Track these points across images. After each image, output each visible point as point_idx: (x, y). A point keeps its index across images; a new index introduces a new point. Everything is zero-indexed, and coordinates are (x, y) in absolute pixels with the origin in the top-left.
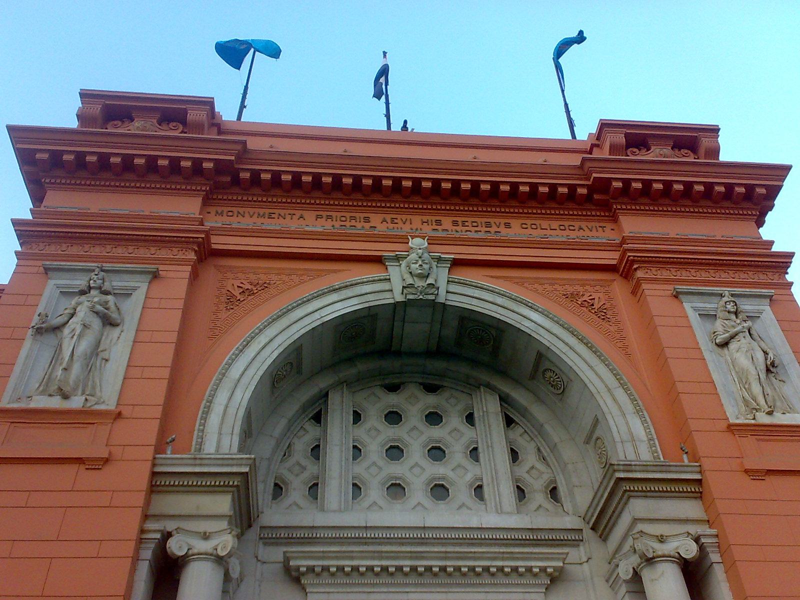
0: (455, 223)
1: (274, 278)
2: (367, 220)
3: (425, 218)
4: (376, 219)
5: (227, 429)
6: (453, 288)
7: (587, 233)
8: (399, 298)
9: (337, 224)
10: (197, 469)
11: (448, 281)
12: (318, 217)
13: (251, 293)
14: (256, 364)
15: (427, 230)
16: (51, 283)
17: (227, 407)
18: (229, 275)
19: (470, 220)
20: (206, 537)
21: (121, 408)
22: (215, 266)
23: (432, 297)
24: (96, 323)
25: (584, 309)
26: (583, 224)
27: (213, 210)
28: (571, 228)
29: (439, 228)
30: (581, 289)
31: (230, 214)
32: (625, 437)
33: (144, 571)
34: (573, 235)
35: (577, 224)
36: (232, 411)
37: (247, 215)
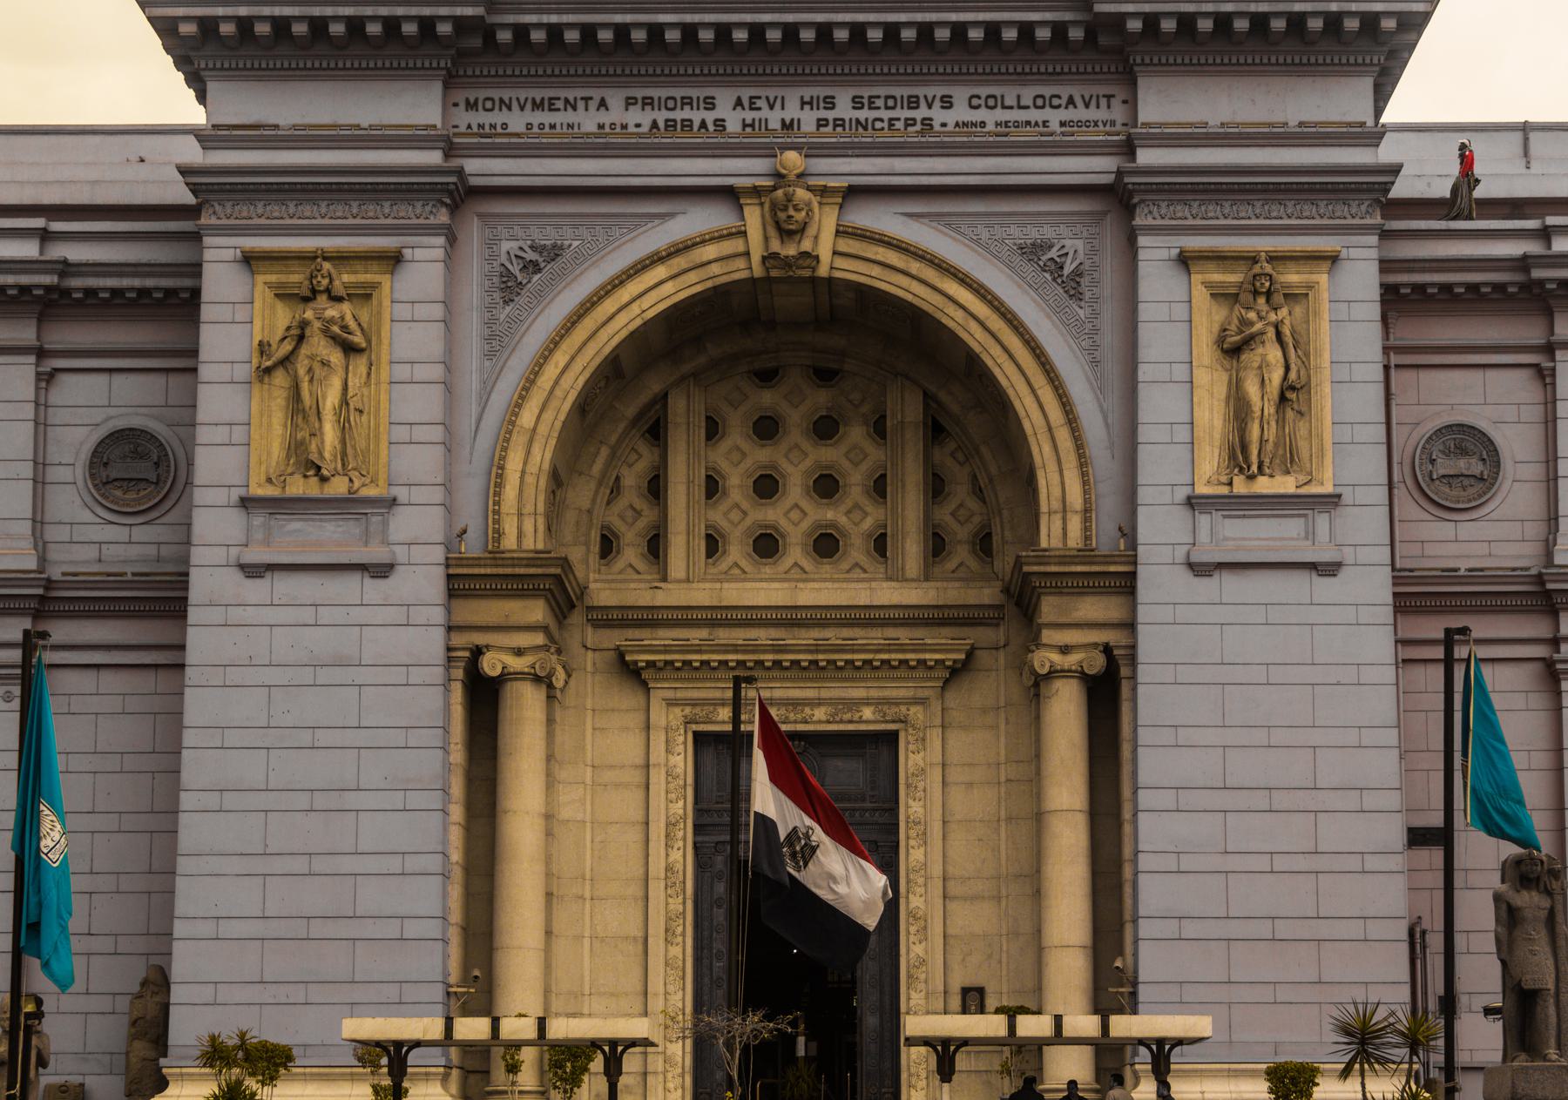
0: (857, 103)
1: (569, 232)
2: (710, 104)
3: (808, 92)
4: (724, 99)
5: (529, 508)
6: (846, 245)
7: (1080, 113)
8: (758, 271)
9: (662, 116)
10: (501, 571)
11: (837, 232)
12: (630, 102)
13: (534, 267)
14: (554, 404)
15: (808, 119)
16: (260, 279)
17: (523, 472)
18: (503, 232)
19: (882, 91)
20: (519, 652)
21: (395, 491)
22: (480, 215)
23: (806, 273)
24: (336, 357)
25: (1047, 275)
26: (1076, 92)
27: (460, 96)
28: (1056, 102)
29: (830, 115)
30: (1048, 232)
31: (489, 105)
32: (1056, 505)
33: (457, 691)
34: (1054, 117)
35: (1065, 91)
36: (530, 479)
37: (515, 104)
